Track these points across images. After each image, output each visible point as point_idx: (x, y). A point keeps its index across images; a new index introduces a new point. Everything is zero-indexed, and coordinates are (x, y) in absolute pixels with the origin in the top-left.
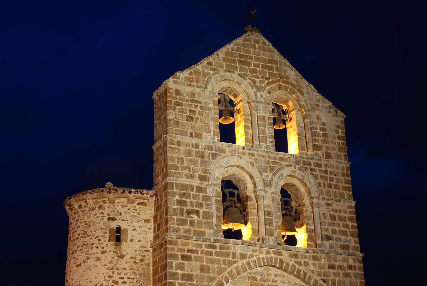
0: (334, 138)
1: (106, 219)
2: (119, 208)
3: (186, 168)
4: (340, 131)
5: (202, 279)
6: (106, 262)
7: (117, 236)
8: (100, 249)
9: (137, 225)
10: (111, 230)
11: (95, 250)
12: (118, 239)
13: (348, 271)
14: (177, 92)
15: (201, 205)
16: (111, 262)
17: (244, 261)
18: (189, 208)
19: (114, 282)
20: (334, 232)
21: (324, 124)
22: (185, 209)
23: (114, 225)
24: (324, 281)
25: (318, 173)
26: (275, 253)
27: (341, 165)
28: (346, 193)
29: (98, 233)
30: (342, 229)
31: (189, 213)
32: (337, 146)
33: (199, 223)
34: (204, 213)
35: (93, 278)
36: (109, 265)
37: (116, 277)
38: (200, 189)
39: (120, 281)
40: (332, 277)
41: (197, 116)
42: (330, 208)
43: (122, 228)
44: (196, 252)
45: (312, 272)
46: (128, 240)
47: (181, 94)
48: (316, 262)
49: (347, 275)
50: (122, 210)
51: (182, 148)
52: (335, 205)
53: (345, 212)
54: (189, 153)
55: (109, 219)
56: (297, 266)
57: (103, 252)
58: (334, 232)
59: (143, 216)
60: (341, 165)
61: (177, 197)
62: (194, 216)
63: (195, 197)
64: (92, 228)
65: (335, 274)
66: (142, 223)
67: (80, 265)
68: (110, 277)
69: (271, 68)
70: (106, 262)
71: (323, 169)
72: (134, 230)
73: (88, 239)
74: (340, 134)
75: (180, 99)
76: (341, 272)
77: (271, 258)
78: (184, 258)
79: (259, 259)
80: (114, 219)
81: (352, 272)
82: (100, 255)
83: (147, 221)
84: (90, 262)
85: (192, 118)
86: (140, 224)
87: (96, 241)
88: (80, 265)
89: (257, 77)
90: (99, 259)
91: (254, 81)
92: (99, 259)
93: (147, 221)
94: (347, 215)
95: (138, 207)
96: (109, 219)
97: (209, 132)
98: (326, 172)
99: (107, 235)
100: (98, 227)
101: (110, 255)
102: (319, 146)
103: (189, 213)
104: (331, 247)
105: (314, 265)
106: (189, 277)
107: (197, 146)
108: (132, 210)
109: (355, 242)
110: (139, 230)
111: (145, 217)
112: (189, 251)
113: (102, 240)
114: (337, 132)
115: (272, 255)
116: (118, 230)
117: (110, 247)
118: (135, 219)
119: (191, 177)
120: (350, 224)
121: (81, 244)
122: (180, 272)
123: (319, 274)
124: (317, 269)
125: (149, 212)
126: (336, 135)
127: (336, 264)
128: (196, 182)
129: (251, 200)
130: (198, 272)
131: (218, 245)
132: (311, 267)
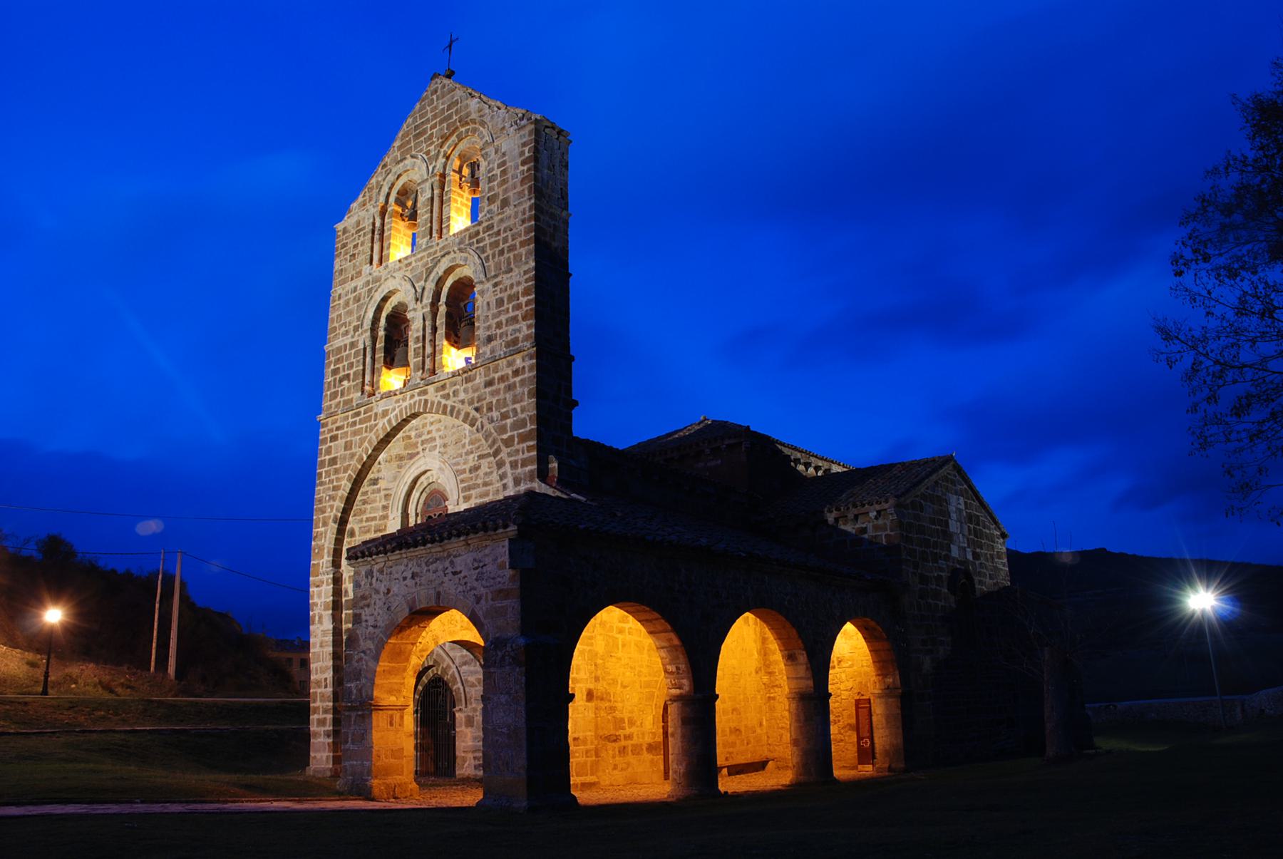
4: (527, 149)
5: (344, 458)
15: (351, 366)
17: (385, 420)
18: (342, 374)
20: (499, 325)
21: (504, 154)
24: (477, 409)
26: (419, 394)
27: (521, 208)
28: (523, 251)
30: (511, 314)
31: (341, 381)
32: (520, 177)
33: (349, 388)
40: (489, 399)
41: (360, 248)
42: (498, 288)
45: (463, 402)
48: (470, 385)
49: (510, 388)
52: (506, 280)
53: (519, 283)
54: (347, 304)
56: (443, 402)
60: (521, 208)
62: (345, 383)
63: (348, 356)
65: (493, 394)
69: (450, 116)
71: (496, 229)
74: (527, 154)
76: (502, 386)
79: (401, 411)
81: (518, 379)
91: (428, 153)
94: (521, 289)
98: (498, 233)
104: (492, 351)
105: (466, 391)
109: (529, 327)
114: (522, 153)
119: (347, 333)
120: (523, 300)
123: (471, 403)
124: (471, 395)
126: (519, 161)
127: (497, 376)
128: (348, 340)
130: (342, 452)
131: (362, 409)
132: (462, 396)
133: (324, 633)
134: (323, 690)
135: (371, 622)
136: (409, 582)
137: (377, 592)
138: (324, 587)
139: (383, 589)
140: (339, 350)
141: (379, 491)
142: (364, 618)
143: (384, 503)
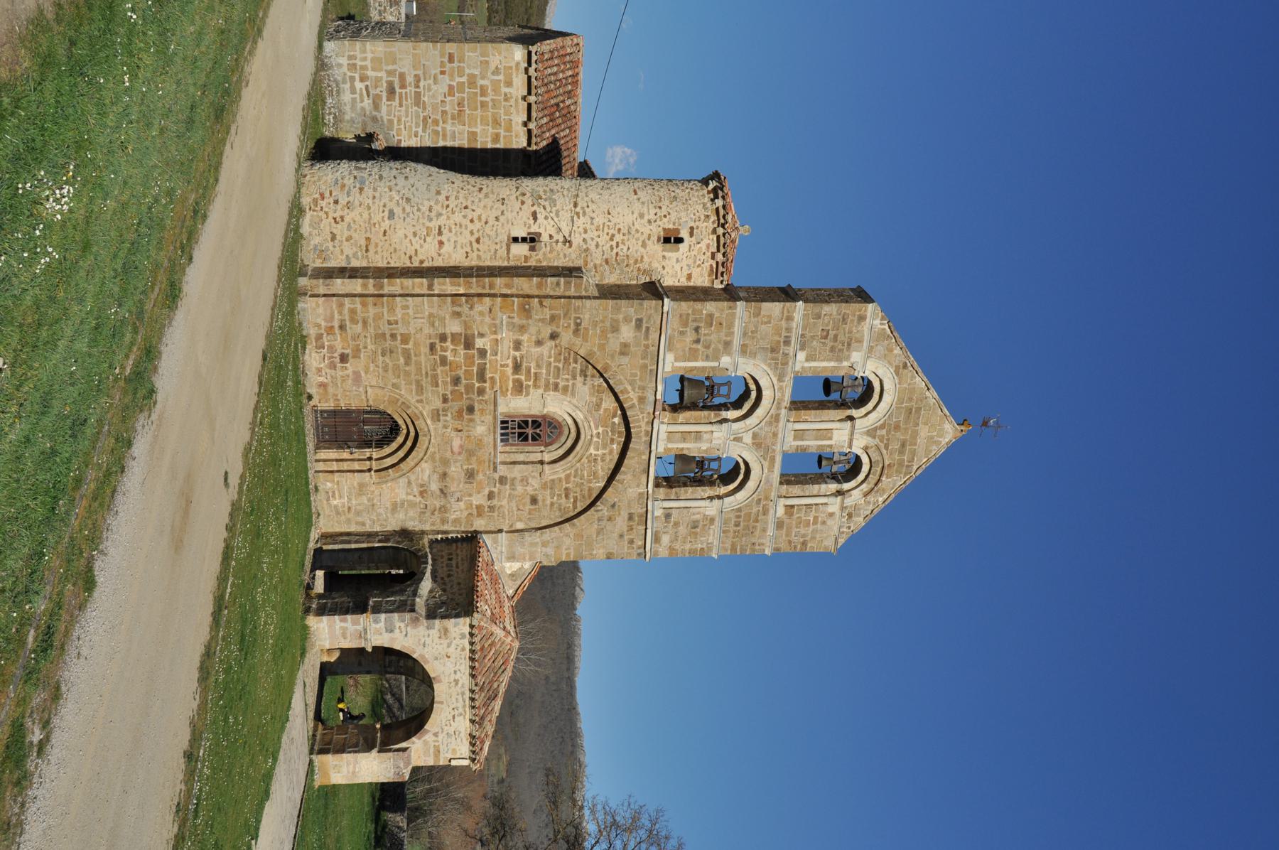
0: (804, 536)
1: (692, 224)
2: (706, 241)
3: (756, 327)
6: (637, 226)
7: (672, 239)
8: (652, 217)
9: (684, 263)
10: (678, 231)
11: (653, 211)
12: (667, 240)
13: (626, 537)
14: (862, 318)
16: (637, 231)
17: (635, 401)
18: (703, 331)
19: (613, 235)
22: (702, 325)
23: (684, 234)
25: (755, 510)
29: (674, 215)
31: (697, 329)
34: (696, 350)
35: (619, 209)
36: (633, 229)
37: (618, 238)
38: (727, 344)
39: (614, 243)
43: (681, 245)
44: (647, 337)
46: (666, 254)
47: (859, 323)
50: (703, 245)
51: (783, 322)
55: (692, 228)
57: (649, 222)
58: (676, 524)
59: (696, 272)
61: (717, 315)
64: (682, 207)
66: (686, 272)
67: (636, 193)
68: (619, 230)
69: (901, 452)
70: (637, 226)
72: (678, 261)
73: (667, 202)
75: (852, 321)
77: (640, 437)
78: (639, 321)
80: (691, 234)
82: (646, 218)
83: (689, 277)
84: (637, 207)
85: (826, 338)
86: (685, 268)
87: (664, 211)
88: (636, 193)
89: (888, 432)
90: (642, 216)
92: (642, 216)
93: (689, 277)
95: (707, 265)
96: (692, 228)
97: (807, 360)
98: (756, 521)
99: (671, 226)
100: (683, 214)
101: (646, 230)
102: (792, 514)
103: (697, 329)
106: (615, 329)
107: (787, 343)
108: (703, 257)
110: (677, 267)
111: (694, 275)
112: (648, 329)
113: (665, 220)
115: (644, 439)
116: (679, 240)
117: (657, 231)
118: (690, 261)
121: (661, 194)
122: (621, 317)
125: (701, 279)
129: (716, 416)
133: (443, 320)
134: (386, 317)
135: (428, 641)
136: (453, 677)
137: (449, 646)
138: (487, 319)
139: (451, 650)
140: (731, 326)
141: (574, 378)
142: (431, 632)
143: (562, 384)
